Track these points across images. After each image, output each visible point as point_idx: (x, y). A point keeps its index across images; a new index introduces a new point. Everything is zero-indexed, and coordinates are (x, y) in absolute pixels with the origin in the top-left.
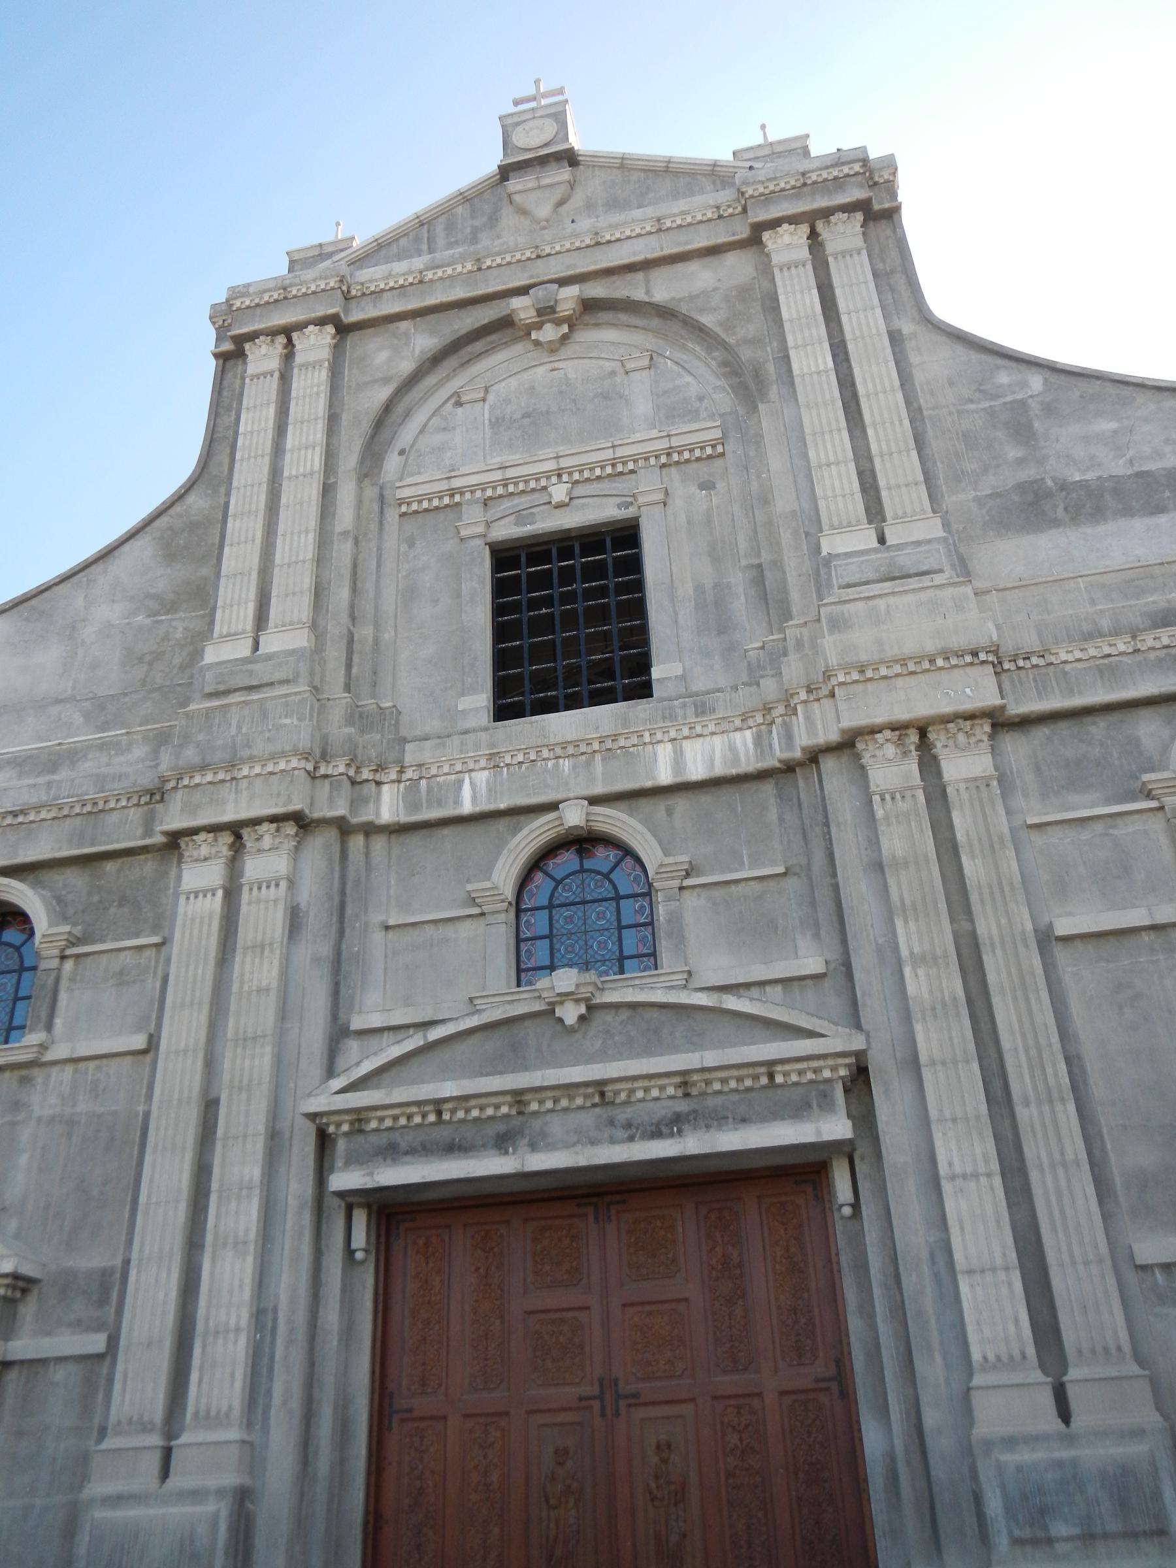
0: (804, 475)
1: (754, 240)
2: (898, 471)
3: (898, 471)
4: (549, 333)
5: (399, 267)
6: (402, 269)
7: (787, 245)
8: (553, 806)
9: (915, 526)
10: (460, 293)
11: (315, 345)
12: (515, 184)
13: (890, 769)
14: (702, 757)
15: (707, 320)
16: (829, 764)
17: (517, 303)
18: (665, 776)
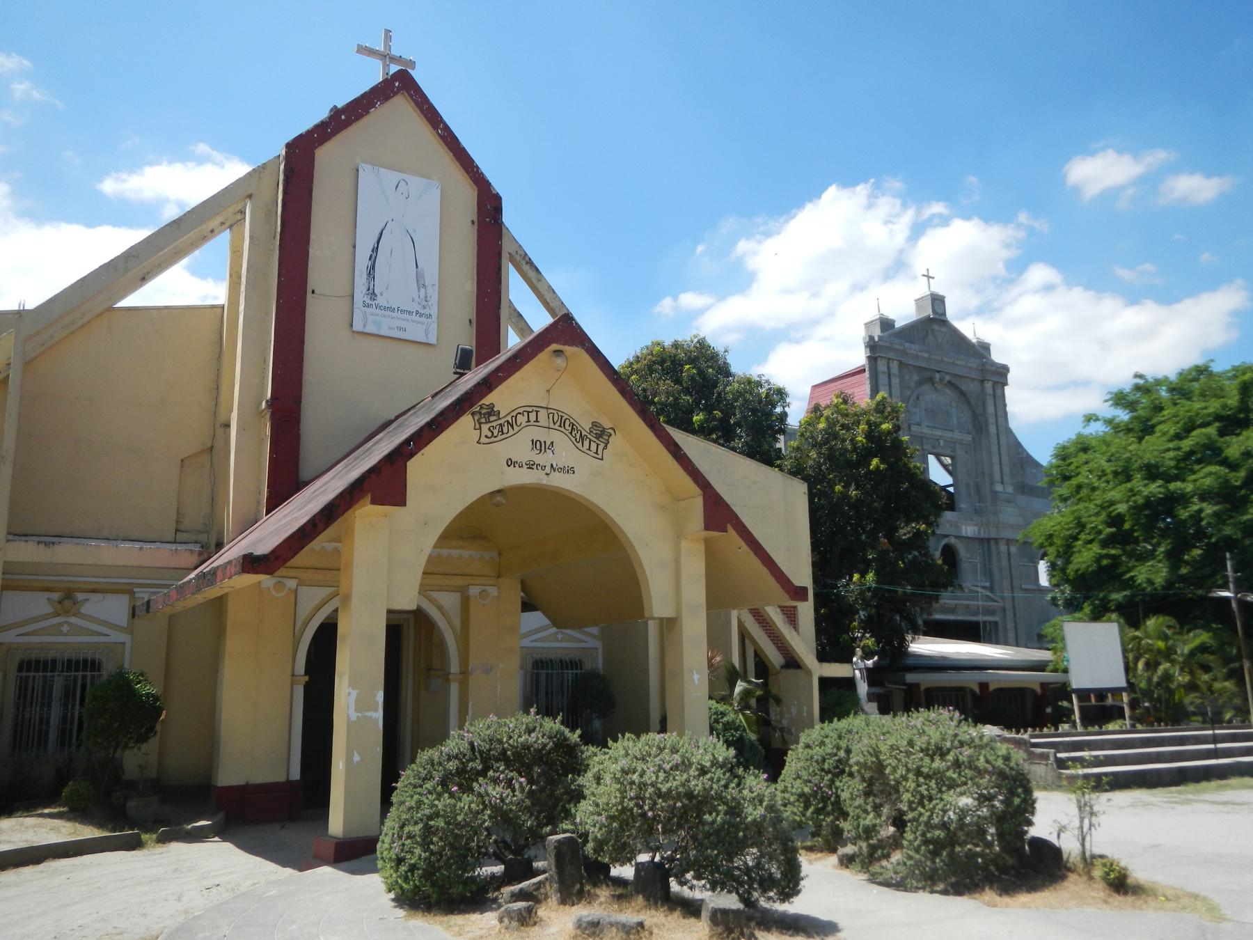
0: (991, 464)
1: (982, 382)
2: (1006, 469)
3: (1006, 469)
4: (939, 387)
5: (913, 346)
6: (913, 348)
7: (988, 385)
8: (947, 536)
9: (1010, 489)
10: (924, 365)
11: (895, 367)
12: (936, 327)
13: (1003, 548)
14: (969, 530)
15: (973, 402)
16: (992, 542)
17: (938, 376)
18: (964, 534)
